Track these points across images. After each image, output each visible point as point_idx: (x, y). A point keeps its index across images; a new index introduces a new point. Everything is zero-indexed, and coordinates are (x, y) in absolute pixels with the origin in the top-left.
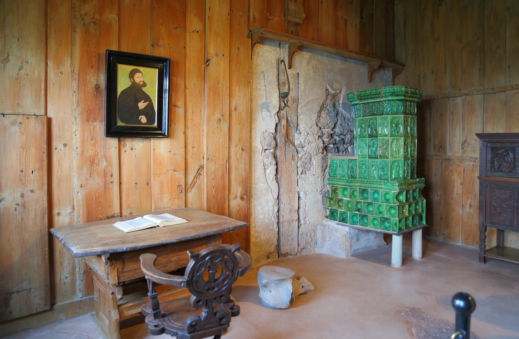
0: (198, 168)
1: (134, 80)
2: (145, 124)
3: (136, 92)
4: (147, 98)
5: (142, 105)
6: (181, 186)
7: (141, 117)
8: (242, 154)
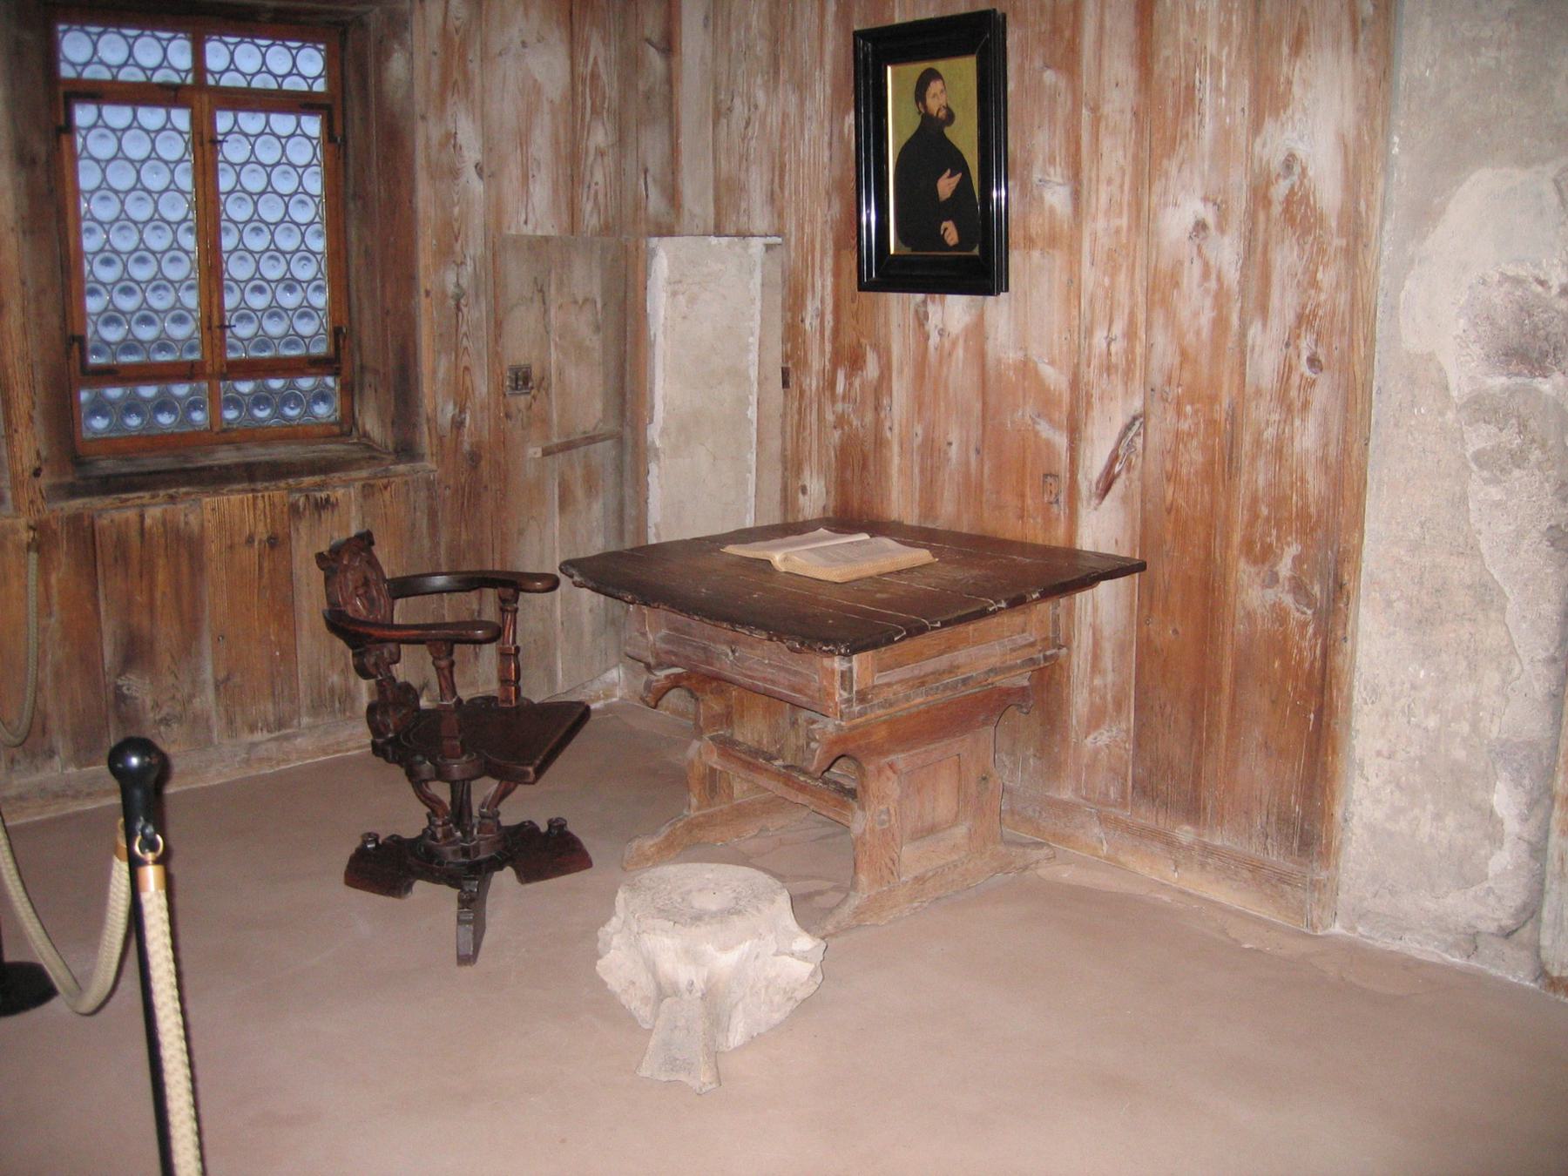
0: (1128, 420)
1: (925, 107)
2: (955, 247)
3: (931, 145)
4: (955, 161)
5: (946, 186)
6: (1056, 476)
7: (945, 224)
8: (1313, 383)
